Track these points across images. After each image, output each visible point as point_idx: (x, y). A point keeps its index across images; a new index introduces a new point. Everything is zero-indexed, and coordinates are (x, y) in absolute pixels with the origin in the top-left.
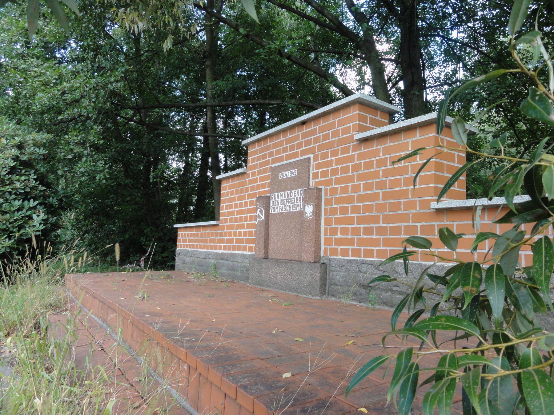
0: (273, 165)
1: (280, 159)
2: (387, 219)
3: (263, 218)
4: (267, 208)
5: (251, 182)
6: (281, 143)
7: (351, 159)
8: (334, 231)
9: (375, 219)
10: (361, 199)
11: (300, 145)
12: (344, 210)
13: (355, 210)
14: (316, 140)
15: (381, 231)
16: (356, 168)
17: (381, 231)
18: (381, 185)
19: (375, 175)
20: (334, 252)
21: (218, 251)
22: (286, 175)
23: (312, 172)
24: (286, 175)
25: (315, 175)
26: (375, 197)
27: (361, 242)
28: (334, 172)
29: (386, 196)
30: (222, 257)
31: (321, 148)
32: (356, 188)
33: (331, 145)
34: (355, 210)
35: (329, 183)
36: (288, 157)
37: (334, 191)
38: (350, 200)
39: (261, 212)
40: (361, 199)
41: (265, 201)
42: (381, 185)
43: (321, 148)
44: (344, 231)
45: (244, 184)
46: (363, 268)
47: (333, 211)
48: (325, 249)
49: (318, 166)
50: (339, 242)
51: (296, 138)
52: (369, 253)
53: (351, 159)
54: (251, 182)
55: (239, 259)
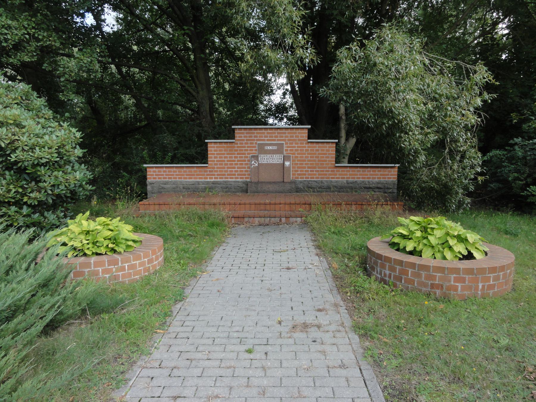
0: (258, 142)
1: (264, 140)
2: (319, 168)
3: (257, 165)
4: (258, 161)
5: (238, 147)
6: (264, 133)
7: (305, 147)
8: (297, 171)
9: (315, 168)
10: (309, 161)
11: (276, 137)
12: (300, 164)
13: (306, 164)
14: (287, 137)
15: (316, 171)
16: (307, 150)
17: (316, 171)
18: (317, 157)
19: (315, 154)
20: (298, 178)
21: (208, 180)
22: (270, 148)
23: (284, 149)
24: (270, 148)
25: (286, 150)
26: (315, 161)
27: (309, 174)
28: (296, 150)
29: (319, 161)
30: (214, 183)
31: (289, 140)
32: (307, 157)
33: (295, 140)
34: (306, 164)
35: (294, 154)
36: (268, 140)
37: (296, 157)
38: (305, 161)
39: (255, 162)
40: (309, 161)
41: (256, 158)
42: (316, 157)
43: (289, 140)
44: (301, 171)
45: (234, 147)
46: (310, 182)
47: (297, 164)
48: (293, 177)
49: (288, 147)
50: (299, 175)
51: (275, 133)
52: (313, 178)
53: (305, 147)
54: (238, 147)
55: (233, 184)
